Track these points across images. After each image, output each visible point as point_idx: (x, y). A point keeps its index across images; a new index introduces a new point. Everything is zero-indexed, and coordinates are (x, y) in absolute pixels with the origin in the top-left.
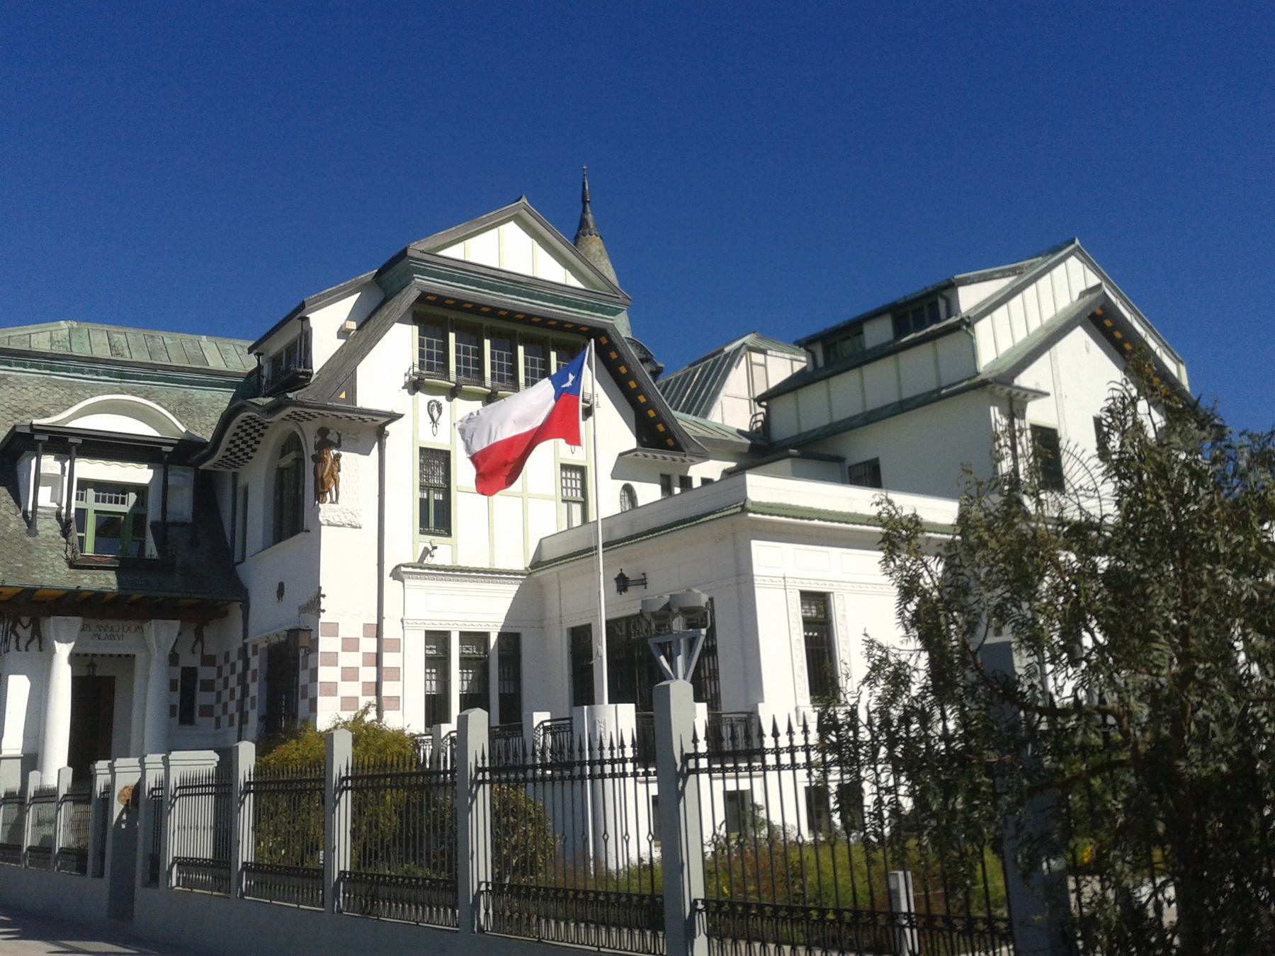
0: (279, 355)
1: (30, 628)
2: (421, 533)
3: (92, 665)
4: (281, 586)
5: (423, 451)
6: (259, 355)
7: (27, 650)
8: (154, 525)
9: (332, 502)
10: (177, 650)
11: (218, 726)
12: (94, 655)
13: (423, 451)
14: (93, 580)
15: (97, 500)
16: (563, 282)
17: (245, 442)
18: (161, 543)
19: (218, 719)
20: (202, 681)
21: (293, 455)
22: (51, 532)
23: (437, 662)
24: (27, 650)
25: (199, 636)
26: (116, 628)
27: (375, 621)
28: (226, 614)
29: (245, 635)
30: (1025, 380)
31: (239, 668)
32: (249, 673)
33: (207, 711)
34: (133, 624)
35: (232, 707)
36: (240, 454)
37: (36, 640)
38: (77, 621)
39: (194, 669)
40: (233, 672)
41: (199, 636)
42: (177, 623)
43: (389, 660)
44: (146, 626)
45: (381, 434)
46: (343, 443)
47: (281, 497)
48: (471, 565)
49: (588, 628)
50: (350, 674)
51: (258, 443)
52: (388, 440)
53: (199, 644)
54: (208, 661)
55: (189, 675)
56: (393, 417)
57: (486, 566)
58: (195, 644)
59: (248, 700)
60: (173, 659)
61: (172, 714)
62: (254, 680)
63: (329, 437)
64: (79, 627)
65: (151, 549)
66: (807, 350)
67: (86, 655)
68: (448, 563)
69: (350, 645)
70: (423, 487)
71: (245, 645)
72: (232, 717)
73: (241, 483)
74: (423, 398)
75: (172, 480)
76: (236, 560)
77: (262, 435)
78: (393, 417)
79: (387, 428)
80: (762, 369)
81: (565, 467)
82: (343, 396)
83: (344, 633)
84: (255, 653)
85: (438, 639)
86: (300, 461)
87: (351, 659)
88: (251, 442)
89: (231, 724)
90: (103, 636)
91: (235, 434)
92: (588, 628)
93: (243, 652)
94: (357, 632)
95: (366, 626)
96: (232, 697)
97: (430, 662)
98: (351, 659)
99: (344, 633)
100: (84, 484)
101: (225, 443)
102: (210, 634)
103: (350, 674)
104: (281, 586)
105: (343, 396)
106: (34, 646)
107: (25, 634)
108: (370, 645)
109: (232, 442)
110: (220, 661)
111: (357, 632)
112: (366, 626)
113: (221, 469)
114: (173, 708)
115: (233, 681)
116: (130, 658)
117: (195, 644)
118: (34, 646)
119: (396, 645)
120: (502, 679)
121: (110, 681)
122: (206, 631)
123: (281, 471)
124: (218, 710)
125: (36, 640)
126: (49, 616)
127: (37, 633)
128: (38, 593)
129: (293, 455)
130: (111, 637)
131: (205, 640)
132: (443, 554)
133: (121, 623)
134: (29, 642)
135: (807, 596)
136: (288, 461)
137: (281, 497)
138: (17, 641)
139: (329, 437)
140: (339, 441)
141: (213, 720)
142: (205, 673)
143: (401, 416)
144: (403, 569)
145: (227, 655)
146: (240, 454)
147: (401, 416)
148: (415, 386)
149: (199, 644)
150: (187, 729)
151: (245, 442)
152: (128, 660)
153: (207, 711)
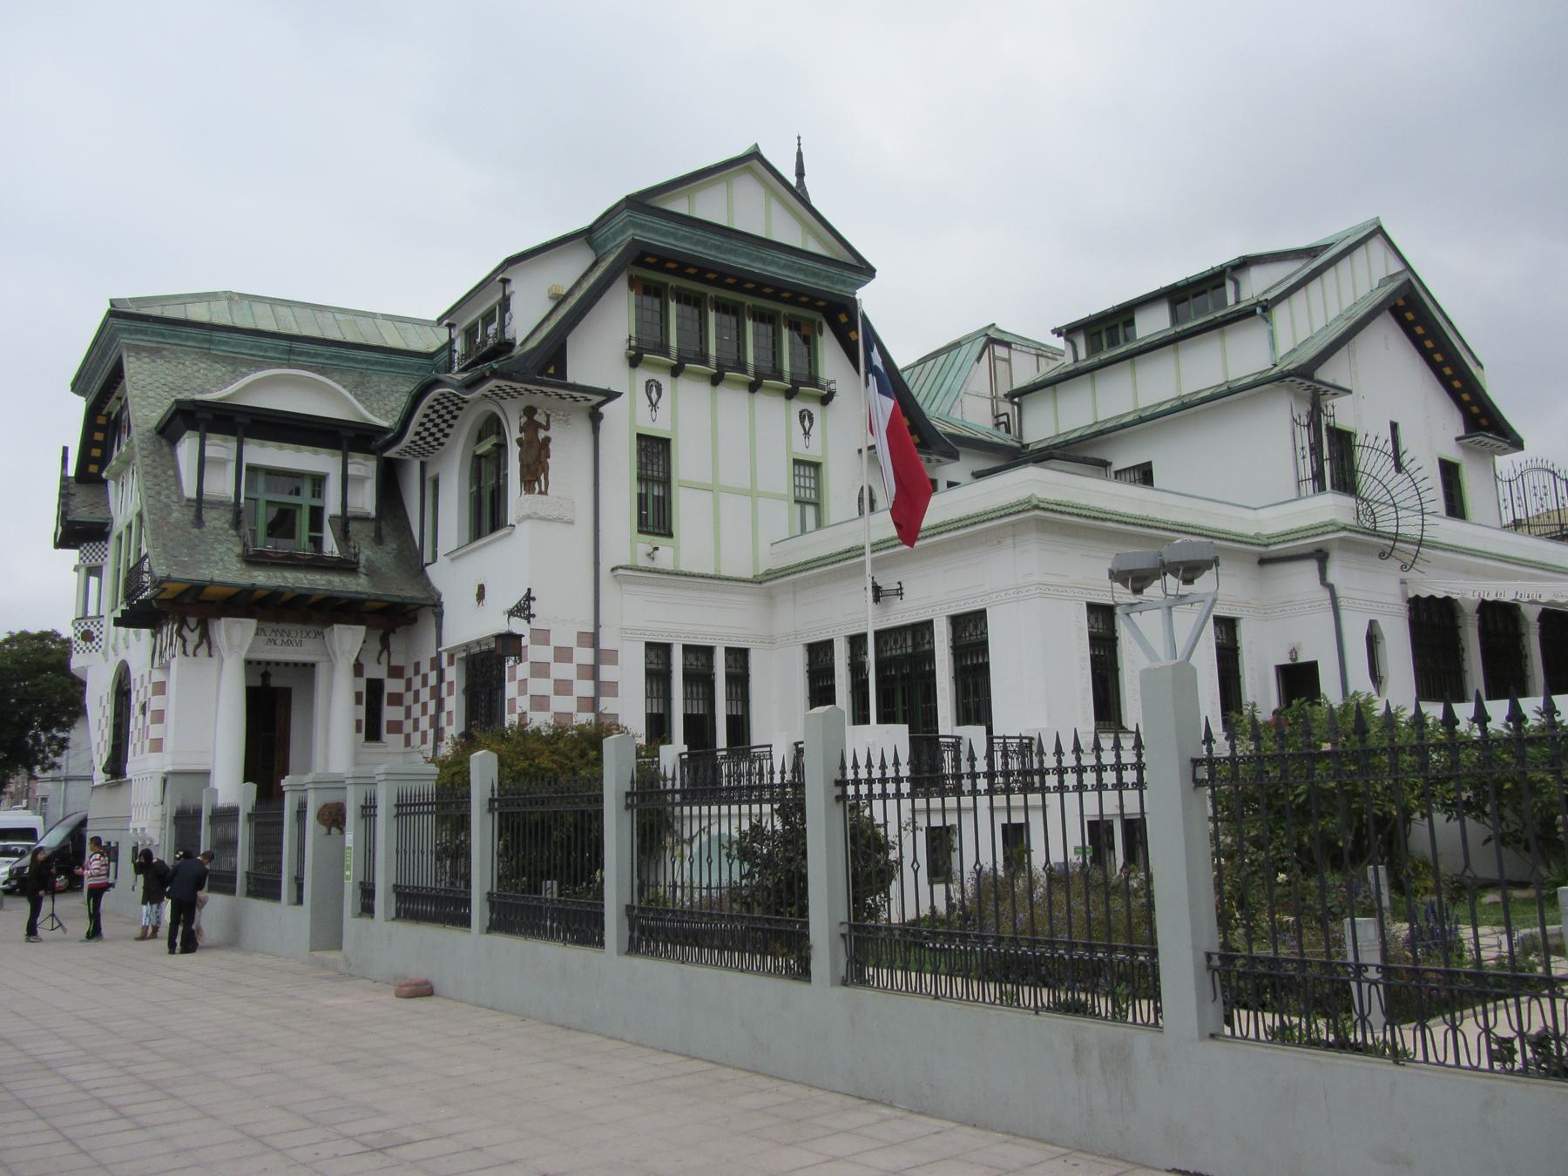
0: (474, 326)
1: (197, 632)
2: (640, 532)
3: (266, 676)
4: (481, 588)
5: (639, 436)
6: (450, 326)
8: (333, 518)
9: (541, 492)
10: (362, 660)
11: (408, 742)
12: (268, 663)
13: (639, 436)
14: (269, 578)
15: (268, 490)
16: (798, 244)
17: (436, 425)
18: (344, 536)
19: (408, 738)
20: (390, 695)
21: (493, 440)
22: (218, 524)
23: (658, 677)
25: (385, 645)
26: (293, 634)
27: (591, 629)
28: (414, 620)
29: (439, 644)
30: (1326, 374)
31: (433, 679)
32: (444, 686)
33: (396, 727)
34: (312, 628)
35: (425, 723)
36: (430, 439)
37: (205, 645)
38: (251, 624)
40: (425, 684)
41: (385, 645)
42: (362, 629)
43: (606, 673)
44: (327, 631)
45: (595, 417)
47: (479, 488)
48: (696, 570)
49: (829, 644)
50: (563, 687)
51: (450, 426)
52: (603, 424)
53: (385, 654)
54: (396, 672)
55: (375, 687)
56: (611, 396)
57: (712, 572)
58: (380, 654)
59: (444, 716)
60: (358, 669)
61: (358, 730)
62: (450, 693)
63: (537, 418)
64: (252, 633)
65: (330, 546)
66: (1067, 339)
67: (259, 663)
68: (670, 567)
69: (563, 654)
70: (640, 479)
71: (439, 654)
72: (424, 734)
73: (430, 474)
74: (643, 375)
75: (352, 470)
76: (426, 561)
77: (455, 417)
78: (611, 396)
79: (602, 409)
80: (1004, 364)
81: (797, 462)
82: (551, 371)
83: (557, 640)
84: (451, 663)
85: (658, 652)
86: (501, 447)
87: (565, 671)
88: (443, 426)
89: (424, 741)
91: (426, 416)
92: (829, 644)
93: (436, 664)
94: (571, 641)
95: (580, 634)
96: (424, 712)
97: (650, 674)
98: (565, 671)
99: (557, 640)
100: (252, 469)
101: (413, 426)
102: (396, 642)
103: (563, 687)
104: (481, 588)
105: (551, 371)
106: (203, 649)
107: (193, 638)
108: (585, 656)
109: (422, 424)
110: (409, 672)
111: (571, 641)
112: (580, 634)
113: (408, 457)
114: (358, 722)
115: (425, 694)
116: (308, 668)
117: (380, 654)
118: (203, 649)
119: (613, 657)
120: (729, 698)
121: (286, 693)
122: (392, 639)
123: (478, 459)
124: (408, 726)
125: (205, 645)
126: (219, 617)
127: (205, 636)
128: (207, 590)
129: (493, 440)
130: (289, 643)
132: (666, 555)
133: (299, 627)
134: (197, 647)
135: (1093, 608)
136: (486, 446)
137: (479, 488)
138: (184, 646)
139: (537, 418)
141: (402, 737)
142: (392, 686)
143: (619, 394)
144: (620, 571)
145: (417, 666)
146: (430, 439)
147: (619, 394)
148: (635, 361)
149: (385, 654)
150: (373, 746)
151: (436, 425)
152: (308, 668)
153: (396, 727)
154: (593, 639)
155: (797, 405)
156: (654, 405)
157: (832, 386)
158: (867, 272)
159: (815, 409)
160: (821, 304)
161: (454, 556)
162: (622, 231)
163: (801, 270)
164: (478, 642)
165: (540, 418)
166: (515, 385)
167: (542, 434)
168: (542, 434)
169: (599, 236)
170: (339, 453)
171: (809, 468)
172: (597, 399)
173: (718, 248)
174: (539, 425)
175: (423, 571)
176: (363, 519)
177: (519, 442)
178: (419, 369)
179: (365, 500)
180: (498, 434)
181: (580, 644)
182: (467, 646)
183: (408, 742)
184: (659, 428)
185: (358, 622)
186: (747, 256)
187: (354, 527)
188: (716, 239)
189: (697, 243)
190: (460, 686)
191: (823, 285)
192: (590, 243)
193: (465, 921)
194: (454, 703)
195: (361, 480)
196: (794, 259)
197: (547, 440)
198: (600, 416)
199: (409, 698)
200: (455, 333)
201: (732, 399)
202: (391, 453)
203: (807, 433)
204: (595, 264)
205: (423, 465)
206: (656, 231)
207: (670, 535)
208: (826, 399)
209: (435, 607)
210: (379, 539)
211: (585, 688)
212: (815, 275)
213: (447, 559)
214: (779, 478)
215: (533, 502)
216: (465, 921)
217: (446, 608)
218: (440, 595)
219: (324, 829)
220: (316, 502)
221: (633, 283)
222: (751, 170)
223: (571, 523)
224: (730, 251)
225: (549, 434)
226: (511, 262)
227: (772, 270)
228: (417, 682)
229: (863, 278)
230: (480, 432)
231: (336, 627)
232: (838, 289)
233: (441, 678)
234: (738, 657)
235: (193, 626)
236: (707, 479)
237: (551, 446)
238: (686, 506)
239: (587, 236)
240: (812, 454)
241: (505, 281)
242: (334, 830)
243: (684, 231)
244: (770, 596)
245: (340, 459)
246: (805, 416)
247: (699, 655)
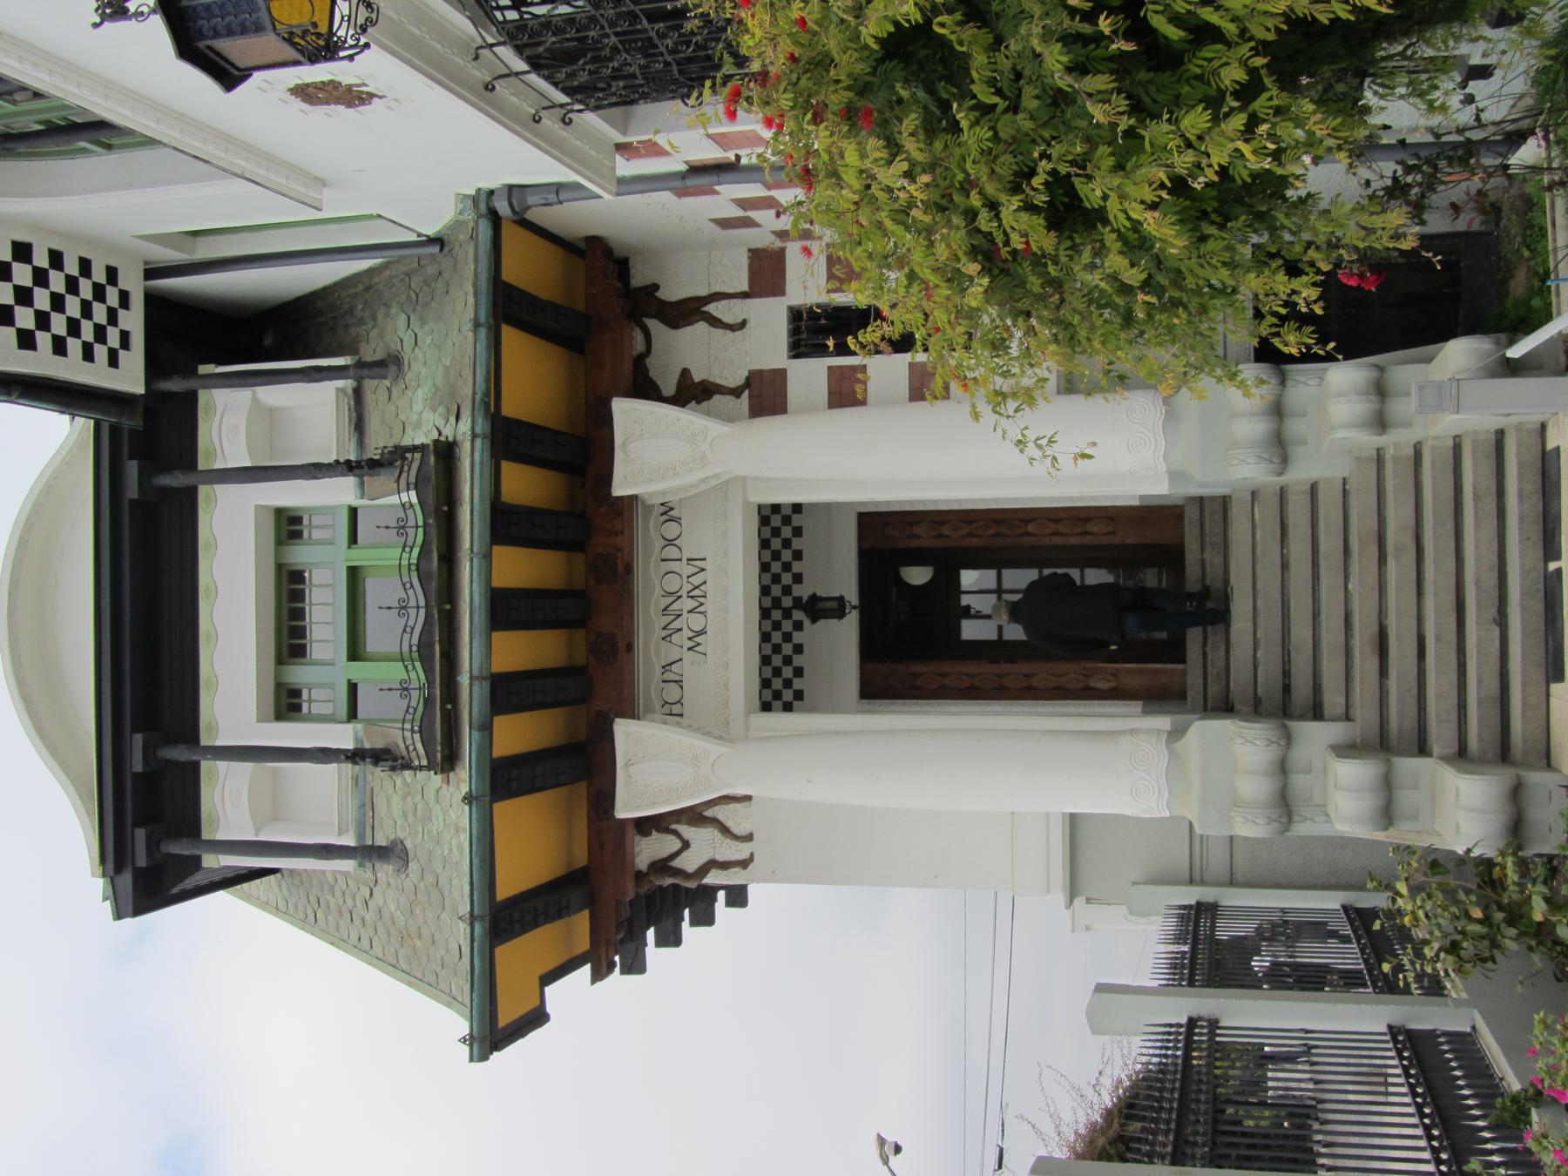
1: (687, 831)
7: (749, 838)
10: (736, 378)
24: (749, 838)
26: (673, 583)
34: (647, 543)
38: (625, 732)
39: (796, 315)
53: (713, 309)
54: (767, 272)
58: (715, 322)
90: (696, 622)
107: (703, 845)
117: (715, 322)
122: (672, 292)
130: (697, 594)
131: (703, 292)
134: (725, 830)
138: (725, 866)
149: (713, 309)
195: (271, 418)
231: (620, 488)
235: (673, 844)
245: (220, 489)
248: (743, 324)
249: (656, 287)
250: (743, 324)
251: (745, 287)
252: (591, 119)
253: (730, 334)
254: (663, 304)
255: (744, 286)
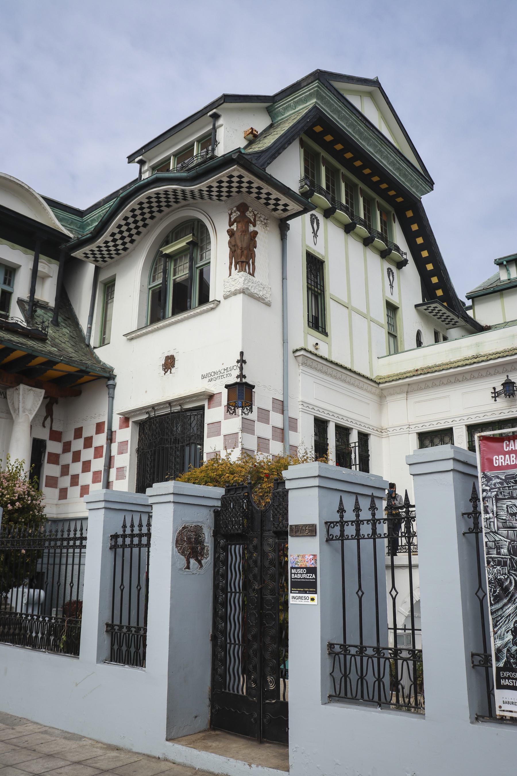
6: (142, 163)
8: (20, 302)
9: (249, 273)
18: (30, 316)
31: (100, 440)
32: (114, 447)
33: (52, 482)
42: (43, 391)
44: (9, 392)
45: (283, 228)
46: (258, 223)
47: (165, 280)
52: (289, 233)
53: (49, 419)
54: (56, 436)
62: (120, 452)
73: (104, 276)
85: (321, 425)
94: (268, 406)
101: (112, 227)
108: (276, 419)
110: (69, 436)
111: (268, 406)
122: (56, 409)
124: (65, 482)
129: (189, 238)
131: (54, 417)
137: (165, 280)
140: (255, 219)
142: (53, 447)
144: (302, 352)
145: (78, 433)
149: (49, 419)
154: (281, 406)
155: (387, 265)
156: (315, 235)
157: (405, 256)
158: (430, 184)
159: (394, 269)
160: (400, 200)
161: (131, 337)
162: (306, 100)
163: (398, 169)
164: (170, 403)
165: (249, 215)
166: (248, 177)
167: (251, 228)
168: (251, 228)
169: (280, 106)
170: (34, 253)
171: (392, 308)
172: (294, 207)
173: (360, 134)
174: (250, 221)
175: (92, 353)
176: (44, 306)
177: (231, 233)
178: (72, 223)
179: (47, 293)
180: (193, 235)
181: (274, 409)
182: (153, 407)
183: (63, 494)
184: (319, 251)
185: (38, 385)
186: (375, 147)
187: (39, 312)
188: (361, 127)
189: (351, 125)
190: (132, 447)
191: (407, 185)
192: (270, 112)
193: (72, 648)
194: (125, 461)
196: (398, 159)
197: (256, 233)
198: (287, 227)
199: (67, 459)
200: (146, 167)
201: (355, 247)
202: (78, 254)
203: (391, 286)
204: (271, 126)
205: (97, 270)
206: (330, 106)
207: (326, 335)
208: (401, 264)
209: (105, 378)
210: (56, 323)
211: (276, 448)
212: (405, 176)
213: (125, 338)
214: (380, 313)
215: (239, 279)
216: (69, 644)
217: (118, 380)
218: (111, 370)
219: (183, 560)
220: (7, 288)
221: (302, 144)
222: (370, 95)
223: (268, 304)
224: (365, 139)
225: (256, 229)
226: (227, 98)
227: (384, 163)
228: (78, 445)
229: (428, 188)
230: (168, 236)
231: (22, 387)
232: (413, 190)
233: (110, 439)
234: (364, 438)
236: (344, 299)
237: (256, 239)
238: (334, 315)
239: (269, 104)
240: (395, 300)
241: (216, 117)
242: (192, 561)
243: (345, 112)
244: (382, 397)
246: (389, 271)
247: (343, 432)
248: (44, 426)
249: (57, 403)
250: (44, 426)
251: (53, 429)
252: (145, 417)
253: (42, 422)
254: (52, 404)
255: (53, 429)
